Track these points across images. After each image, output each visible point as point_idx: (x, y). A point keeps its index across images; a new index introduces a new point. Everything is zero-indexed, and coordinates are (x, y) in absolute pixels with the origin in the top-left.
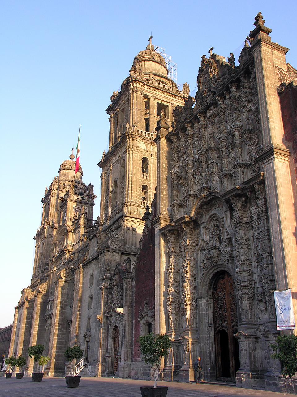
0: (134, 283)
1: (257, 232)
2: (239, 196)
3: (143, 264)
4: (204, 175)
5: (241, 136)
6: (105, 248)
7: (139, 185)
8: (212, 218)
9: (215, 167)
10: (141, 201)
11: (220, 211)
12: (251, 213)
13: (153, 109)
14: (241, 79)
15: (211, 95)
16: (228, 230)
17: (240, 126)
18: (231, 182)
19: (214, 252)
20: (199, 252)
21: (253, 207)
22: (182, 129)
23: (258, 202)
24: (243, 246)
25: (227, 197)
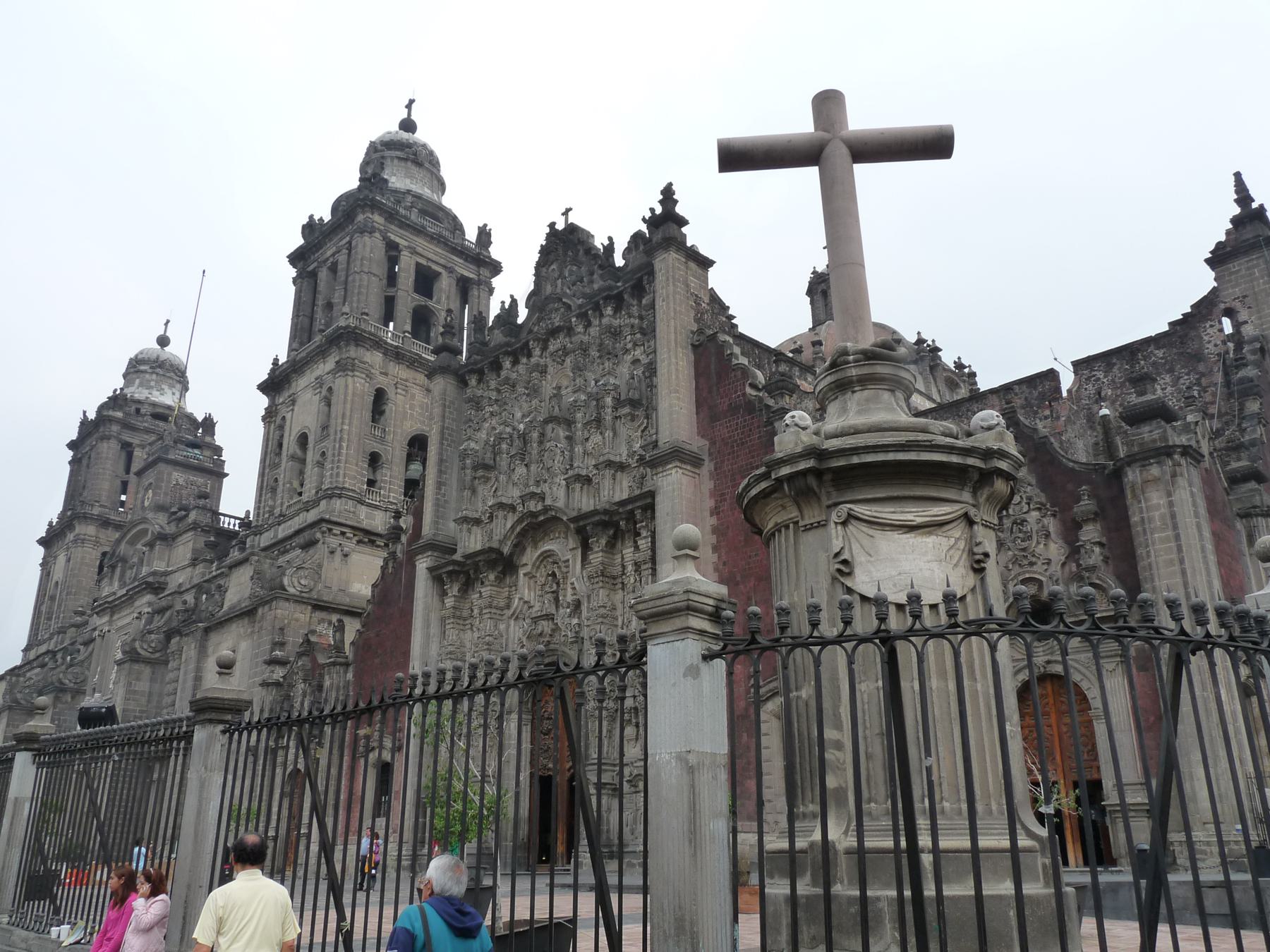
0: (350, 676)
1: (631, 596)
2: (605, 525)
3: (378, 636)
4: (533, 467)
5: (615, 408)
6: (272, 592)
7: (364, 452)
8: (545, 558)
9: (558, 458)
10: (365, 487)
11: (562, 546)
12: (623, 558)
13: (406, 279)
14: (626, 296)
15: (562, 310)
16: (576, 585)
17: (616, 387)
18: (588, 492)
19: (545, 626)
20: (512, 622)
21: (627, 548)
22: (491, 363)
23: (639, 543)
24: (605, 621)
25: (581, 523)
